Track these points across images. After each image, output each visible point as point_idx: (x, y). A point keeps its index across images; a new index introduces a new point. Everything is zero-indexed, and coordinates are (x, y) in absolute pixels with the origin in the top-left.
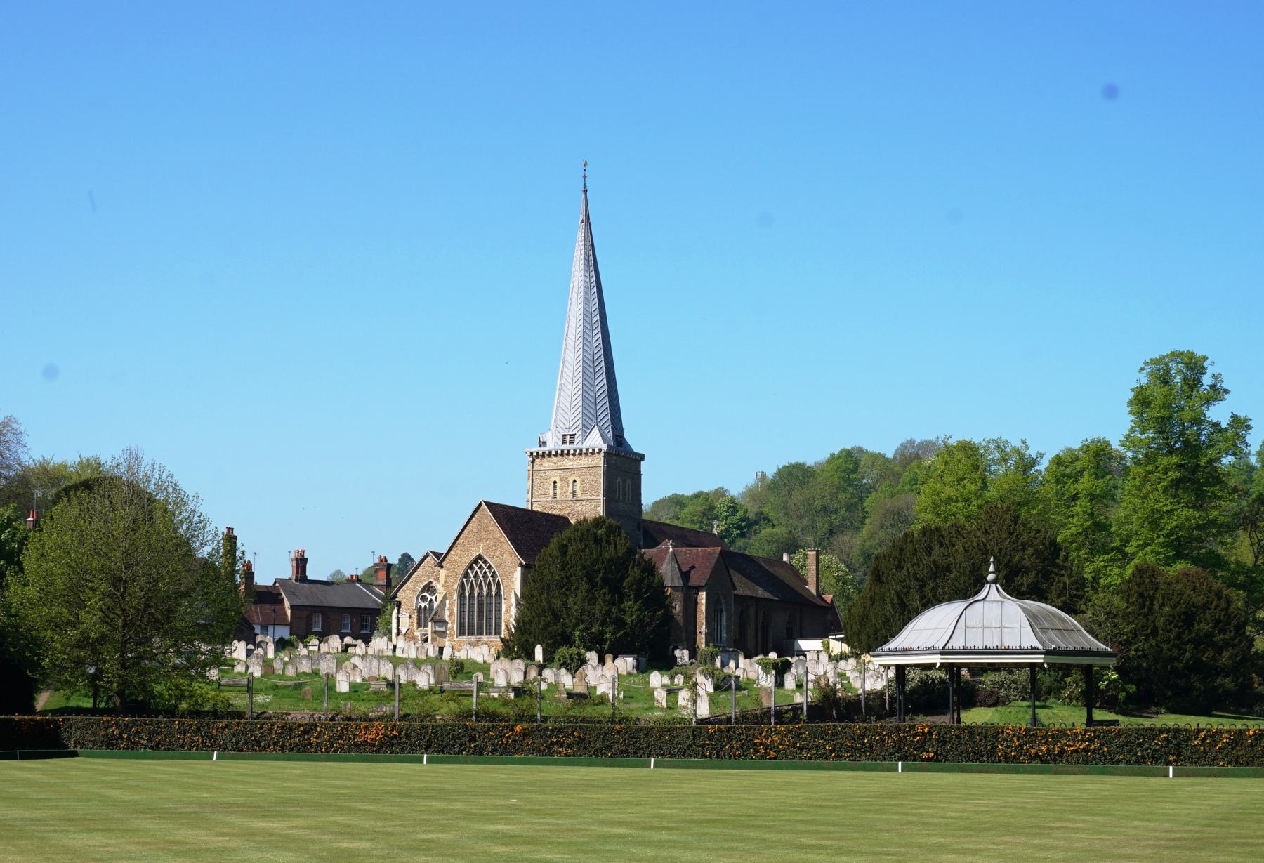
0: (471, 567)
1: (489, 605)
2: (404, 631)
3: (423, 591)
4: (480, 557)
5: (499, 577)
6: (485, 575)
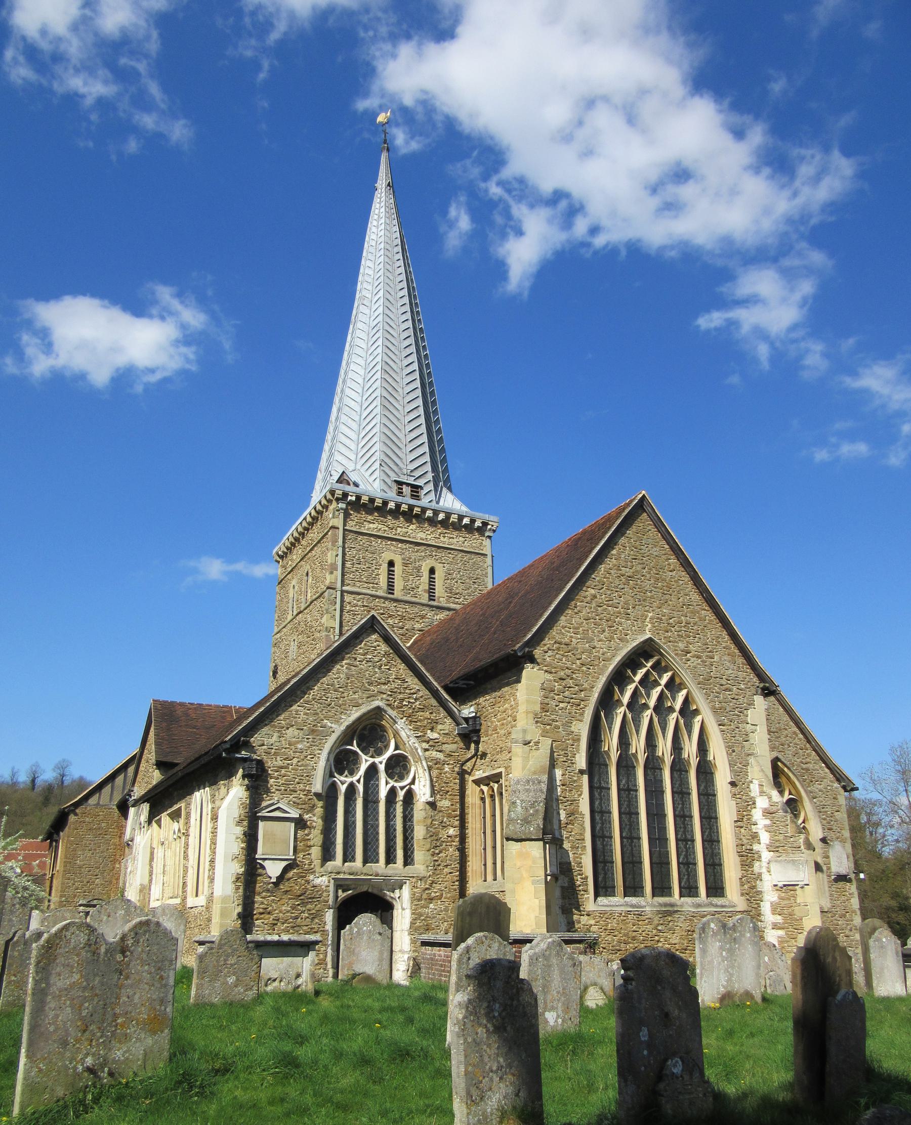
0: (619, 678)
1: (681, 793)
2: (274, 869)
3: (349, 735)
4: (646, 651)
5: (706, 716)
6: (661, 709)
